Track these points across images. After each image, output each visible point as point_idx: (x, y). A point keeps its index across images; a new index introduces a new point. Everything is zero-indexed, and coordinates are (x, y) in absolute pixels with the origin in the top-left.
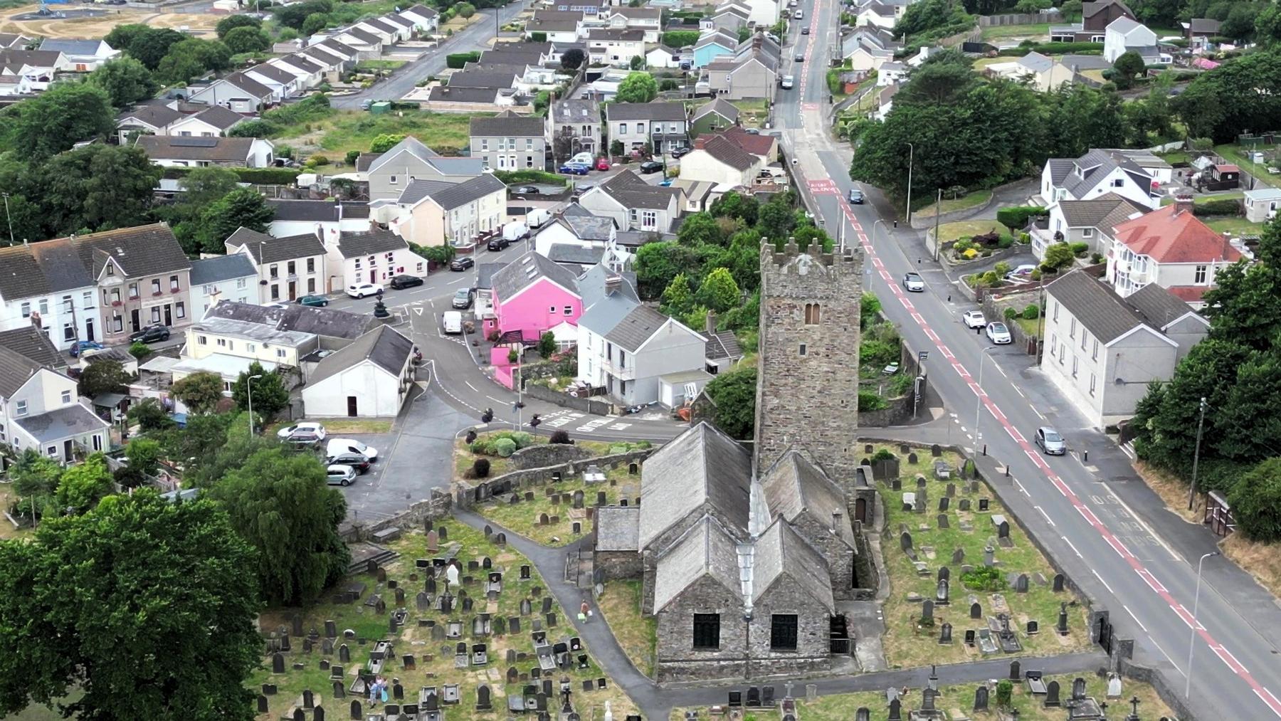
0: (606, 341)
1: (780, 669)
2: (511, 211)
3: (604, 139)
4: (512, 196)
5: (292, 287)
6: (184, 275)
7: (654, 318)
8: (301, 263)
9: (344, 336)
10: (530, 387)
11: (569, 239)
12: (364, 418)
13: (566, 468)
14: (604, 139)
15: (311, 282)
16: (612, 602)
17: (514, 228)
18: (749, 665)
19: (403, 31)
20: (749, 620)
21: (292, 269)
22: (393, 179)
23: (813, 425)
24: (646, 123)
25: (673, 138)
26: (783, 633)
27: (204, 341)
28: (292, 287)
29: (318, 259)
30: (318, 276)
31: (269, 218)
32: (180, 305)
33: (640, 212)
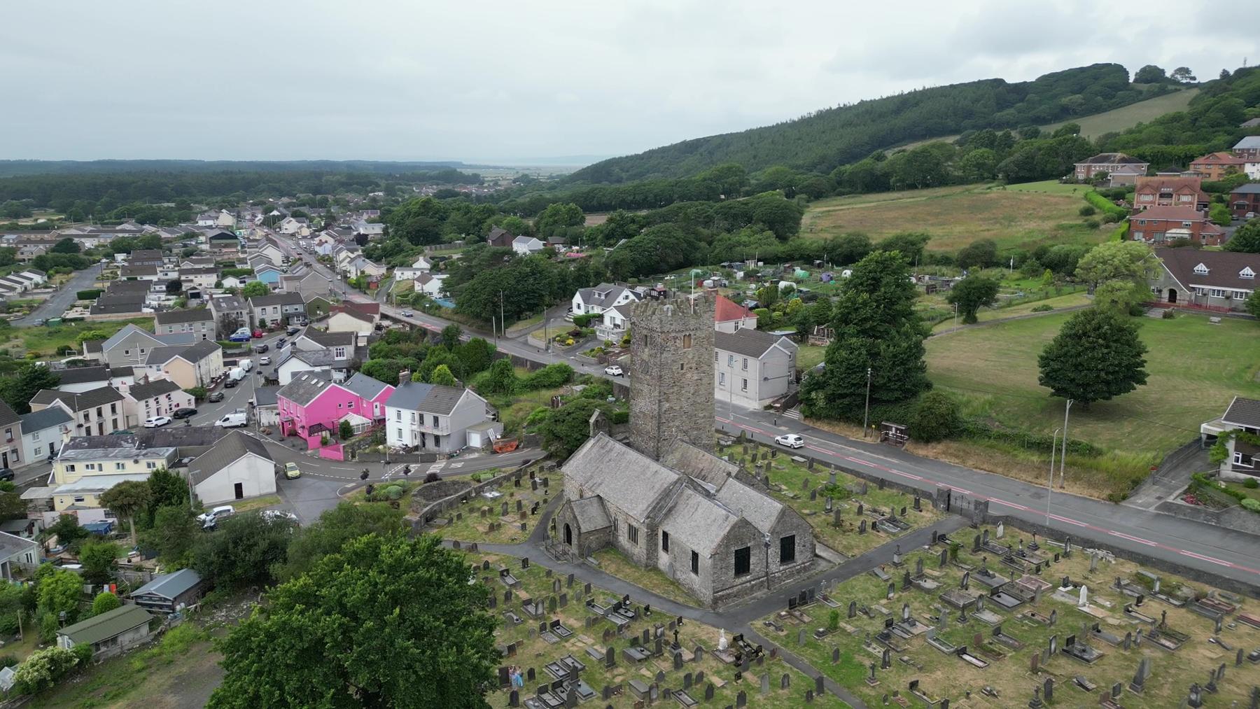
1: (787, 577)
2: (226, 364)
3: (252, 318)
4: (225, 355)
5: (101, 426)
6: (17, 427)
7: (452, 392)
8: (106, 408)
11: (307, 368)
12: (249, 498)
13: (469, 493)
14: (252, 318)
15: (115, 421)
16: (609, 565)
17: (235, 373)
18: (769, 580)
19: (27, 283)
20: (767, 545)
21: (100, 414)
23: (690, 417)
24: (279, 307)
25: (298, 315)
26: (787, 553)
27: (73, 468)
28: (101, 426)
29: (118, 404)
30: (120, 416)
31: (57, 382)
32: (15, 451)
33: (333, 349)
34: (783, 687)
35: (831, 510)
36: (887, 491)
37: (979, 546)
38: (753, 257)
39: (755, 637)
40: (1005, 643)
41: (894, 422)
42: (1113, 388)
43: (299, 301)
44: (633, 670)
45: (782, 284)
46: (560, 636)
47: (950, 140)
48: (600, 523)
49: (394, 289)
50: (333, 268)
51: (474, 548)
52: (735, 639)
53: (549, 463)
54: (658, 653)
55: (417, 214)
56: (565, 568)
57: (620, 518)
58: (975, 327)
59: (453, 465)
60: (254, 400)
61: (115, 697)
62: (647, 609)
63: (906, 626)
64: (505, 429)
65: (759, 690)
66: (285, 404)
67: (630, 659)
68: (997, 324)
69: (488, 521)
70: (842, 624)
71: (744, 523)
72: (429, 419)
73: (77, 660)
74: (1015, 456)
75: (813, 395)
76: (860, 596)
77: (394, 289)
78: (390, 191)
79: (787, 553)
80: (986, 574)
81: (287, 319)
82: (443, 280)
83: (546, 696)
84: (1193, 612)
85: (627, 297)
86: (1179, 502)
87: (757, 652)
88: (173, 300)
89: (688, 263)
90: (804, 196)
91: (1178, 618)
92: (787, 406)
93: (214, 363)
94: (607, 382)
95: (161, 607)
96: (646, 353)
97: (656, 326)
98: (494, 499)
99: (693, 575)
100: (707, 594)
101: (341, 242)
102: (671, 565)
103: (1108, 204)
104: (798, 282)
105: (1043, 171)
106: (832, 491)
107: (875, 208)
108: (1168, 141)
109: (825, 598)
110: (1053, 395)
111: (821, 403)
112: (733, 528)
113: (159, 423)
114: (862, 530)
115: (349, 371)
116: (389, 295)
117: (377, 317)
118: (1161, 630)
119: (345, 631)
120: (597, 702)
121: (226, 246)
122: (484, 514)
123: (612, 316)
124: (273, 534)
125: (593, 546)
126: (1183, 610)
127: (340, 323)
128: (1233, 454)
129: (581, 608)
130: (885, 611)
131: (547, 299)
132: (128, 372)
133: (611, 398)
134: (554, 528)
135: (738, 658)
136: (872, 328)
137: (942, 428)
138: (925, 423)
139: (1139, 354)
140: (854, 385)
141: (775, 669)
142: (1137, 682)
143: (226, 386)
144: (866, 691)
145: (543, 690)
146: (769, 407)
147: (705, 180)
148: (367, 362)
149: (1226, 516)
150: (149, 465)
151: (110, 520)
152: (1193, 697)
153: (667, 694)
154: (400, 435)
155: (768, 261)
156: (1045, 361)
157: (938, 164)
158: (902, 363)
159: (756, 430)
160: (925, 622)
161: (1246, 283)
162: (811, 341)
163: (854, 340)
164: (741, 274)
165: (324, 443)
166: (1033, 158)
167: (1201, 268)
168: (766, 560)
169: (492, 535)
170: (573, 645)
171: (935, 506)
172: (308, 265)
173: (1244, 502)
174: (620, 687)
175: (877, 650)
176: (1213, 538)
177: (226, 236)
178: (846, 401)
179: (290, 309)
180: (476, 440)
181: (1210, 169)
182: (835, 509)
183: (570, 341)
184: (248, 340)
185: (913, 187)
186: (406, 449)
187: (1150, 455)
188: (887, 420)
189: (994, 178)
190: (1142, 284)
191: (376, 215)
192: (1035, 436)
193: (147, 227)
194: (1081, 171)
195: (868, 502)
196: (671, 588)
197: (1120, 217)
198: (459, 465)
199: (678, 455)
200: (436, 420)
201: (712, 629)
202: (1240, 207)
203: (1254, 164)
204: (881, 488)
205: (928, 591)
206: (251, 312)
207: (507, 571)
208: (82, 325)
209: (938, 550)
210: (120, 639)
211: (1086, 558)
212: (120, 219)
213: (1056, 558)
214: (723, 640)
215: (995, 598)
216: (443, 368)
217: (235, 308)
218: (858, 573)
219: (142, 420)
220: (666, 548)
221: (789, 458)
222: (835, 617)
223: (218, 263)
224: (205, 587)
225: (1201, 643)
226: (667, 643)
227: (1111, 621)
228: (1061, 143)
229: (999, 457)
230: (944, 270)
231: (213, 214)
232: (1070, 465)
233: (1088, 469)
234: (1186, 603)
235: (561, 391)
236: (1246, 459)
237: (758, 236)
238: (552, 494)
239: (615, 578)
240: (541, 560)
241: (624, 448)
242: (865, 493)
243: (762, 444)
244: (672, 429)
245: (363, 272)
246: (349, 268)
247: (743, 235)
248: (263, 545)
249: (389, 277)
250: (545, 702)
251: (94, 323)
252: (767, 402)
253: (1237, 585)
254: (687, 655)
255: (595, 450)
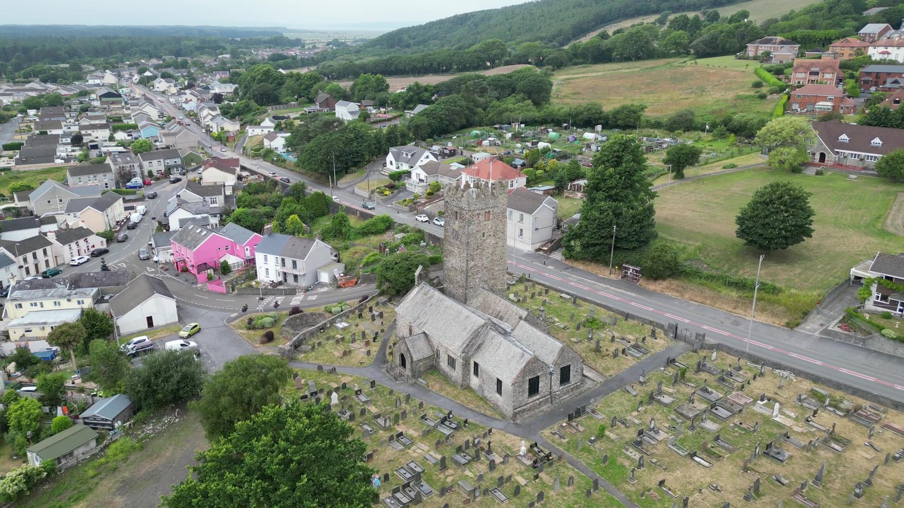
0: (280, 258)
1: (564, 394)
2: (126, 209)
4: (125, 201)
5: (36, 266)
7: (305, 242)
8: (40, 252)
9: (118, 285)
10: (238, 289)
11: (190, 216)
12: (158, 327)
13: (325, 324)
15: (47, 262)
16: (434, 384)
17: (135, 217)
18: (552, 396)
20: (551, 374)
21: (35, 256)
22: (49, 202)
23: (489, 270)
24: (162, 160)
25: (177, 167)
26: (565, 376)
27: (20, 306)
28: (36, 266)
29: (48, 248)
33: (208, 198)
34: (569, 485)
35: (592, 339)
36: (631, 322)
37: (700, 368)
38: (517, 121)
39: (545, 444)
40: (723, 447)
41: (632, 265)
42: (790, 241)
43: (178, 156)
44: (459, 471)
45: (541, 145)
46: (404, 445)
47: (652, 18)
48: (427, 352)
49: (248, 144)
50: (198, 123)
51: (333, 371)
52: (531, 446)
53: (383, 299)
54: (476, 458)
55: (260, 81)
56: (402, 387)
57: (441, 350)
58: (682, 182)
59: (310, 298)
60: (152, 242)
61: (77, 500)
62: (466, 422)
63: (652, 433)
64: (346, 268)
65: (552, 488)
66: (175, 247)
67: (457, 463)
68: (698, 179)
69: (342, 347)
70: (607, 433)
71: (536, 360)
72: (289, 262)
73: (45, 474)
74: (720, 292)
75: (572, 243)
76: (618, 409)
77: (248, 144)
78: (234, 54)
79: (565, 376)
80: (706, 391)
81: (169, 170)
82: (286, 139)
83: (398, 495)
84: (853, 421)
85: (427, 157)
86: (837, 329)
87: (548, 456)
88: (78, 153)
89: (470, 125)
90: (550, 67)
91: (844, 426)
92: (552, 250)
93: (118, 210)
94: (420, 231)
95: (104, 425)
96: (456, 225)
97: (464, 206)
98: (344, 329)
99: (498, 395)
100: (508, 410)
101: (202, 101)
102: (480, 386)
103: (772, 78)
104: (552, 142)
105: (723, 48)
106: (592, 323)
107: (603, 77)
108: (813, 27)
109: (593, 412)
110: (745, 244)
111: (578, 249)
112: (528, 363)
113: (81, 261)
114: (615, 355)
115: (221, 216)
116: (244, 148)
117: (238, 169)
118: (832, 436)
119: (265, 491)
120: (436, 499)
121: (113, 103)
122: (338, 342)
123: (418, 173)
124: (184, 368)
125: (422, 369)
126: (845, 420)
127: (211, 176)
128: (875, 294)
129: (417, 420)
130: (636, 421)
131: (367, 157)
132: (52, 220)
133: (423, 244)
134: (391, 353)
135: (535, 462)
136: (616, 194)
137: (666, 269)
138: (655, 266)
139: (809, 217)
140: (603, 237)
141: (562, 470)
142: (818, 479)
143: (128, 228)
144: (628, 487)
145: (396, 491)
146: (539, 250)
147: (475, 51)
148: (238, 211)
149: (870, 341)
150: (79, 303)
151: (54, 348)
152: (857, 491)
153: (486, 492)
154: (267, 273)
155: (528, 123)
156: (741, 220)
157: (647, 42)
158: (638, 222)
159: (532, 269)
160: (665, 430)
161: (875, 150)
162: (566, 194)
163: (603, 203)
164: (509, 135)
165: (210, 278)
166: (717, 39)
167: (844, 137)
168: (550, 384)
169: (345, 358)
170: (414, 451)
171: (666, 333)
172: (180, 123)
173: (883, 332)
174: (452, 487)
175: (635, 455)
176: (860, 357)
177: (112, 95)
178: (597, 248)
179: (171, 162)
180: (325, 278)
181: (842, 51)
182: (596, 337)
183: (387, 193)
184: (140, 187)
185: (628, 59)
186: (274, 285)
187: (815, 293)
188: (627, 263)
189: (688, 54)
190: (802, 150)
191: (226, 75)
192: (735, 278)
193: (49, 85)
194: (751, 50)
195: (618, 331)
196: (481, 403)
197: (781, 90)
198: (314, 298)
199: (480, 299)
200: (294, 263)
201: (514, 437)
202: (866, 82)
203: (875, 47)
204: (626, 320)
205: (666, 405)
206: (141, 167)
207: (360, 391)
208: (10, 175)
209: (671, 371)
210: (75, 453)
211: (775, 376)
212: (28, 78)
213: (755, 378)
214: (523, 447)
215: (714, 410)
216: (294, 217)
217: (128, 162)
218: (615, 390)
219: (67, 260)
220: (476, 373)
221: (558, 295)
222: (603, 429)
223: (109, 118)
224: (135, 409)
225: (859, 446)
226: (482, 449)
227: (796, 429)
228: (737, 28)
229: (708, 292)
230: (657, 132)
231: (99, 73)
232: (759, 299)
233: (770, 302)
234: (848, 413)
235: (387, 237)
236: (884, 298)
237: (521, 104)
238: (387, 325)
239: (439, 399)
240: (385, 383)
241: (442, 296)
242: (615, 324)
243: (537, 283)
244: (476, 280)
245: (222, 129)
246: (211, 123)
247: (510, 102)
248: (177, 377)
249: (242, 132)
250: (398, 500)
251: (19, 172)
252: (537, 246)
253: (882, 400)
254: (498, 460)
255: (419, 296)
